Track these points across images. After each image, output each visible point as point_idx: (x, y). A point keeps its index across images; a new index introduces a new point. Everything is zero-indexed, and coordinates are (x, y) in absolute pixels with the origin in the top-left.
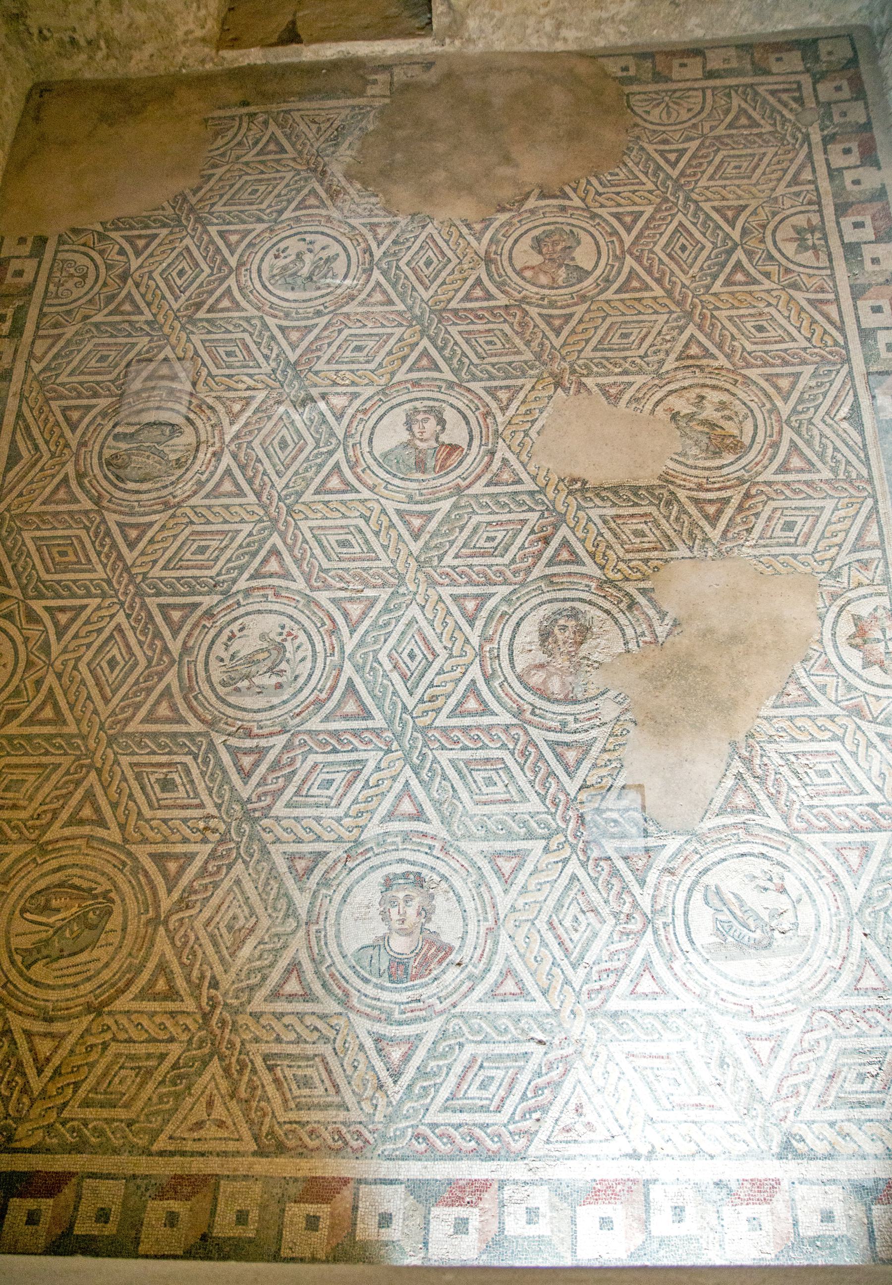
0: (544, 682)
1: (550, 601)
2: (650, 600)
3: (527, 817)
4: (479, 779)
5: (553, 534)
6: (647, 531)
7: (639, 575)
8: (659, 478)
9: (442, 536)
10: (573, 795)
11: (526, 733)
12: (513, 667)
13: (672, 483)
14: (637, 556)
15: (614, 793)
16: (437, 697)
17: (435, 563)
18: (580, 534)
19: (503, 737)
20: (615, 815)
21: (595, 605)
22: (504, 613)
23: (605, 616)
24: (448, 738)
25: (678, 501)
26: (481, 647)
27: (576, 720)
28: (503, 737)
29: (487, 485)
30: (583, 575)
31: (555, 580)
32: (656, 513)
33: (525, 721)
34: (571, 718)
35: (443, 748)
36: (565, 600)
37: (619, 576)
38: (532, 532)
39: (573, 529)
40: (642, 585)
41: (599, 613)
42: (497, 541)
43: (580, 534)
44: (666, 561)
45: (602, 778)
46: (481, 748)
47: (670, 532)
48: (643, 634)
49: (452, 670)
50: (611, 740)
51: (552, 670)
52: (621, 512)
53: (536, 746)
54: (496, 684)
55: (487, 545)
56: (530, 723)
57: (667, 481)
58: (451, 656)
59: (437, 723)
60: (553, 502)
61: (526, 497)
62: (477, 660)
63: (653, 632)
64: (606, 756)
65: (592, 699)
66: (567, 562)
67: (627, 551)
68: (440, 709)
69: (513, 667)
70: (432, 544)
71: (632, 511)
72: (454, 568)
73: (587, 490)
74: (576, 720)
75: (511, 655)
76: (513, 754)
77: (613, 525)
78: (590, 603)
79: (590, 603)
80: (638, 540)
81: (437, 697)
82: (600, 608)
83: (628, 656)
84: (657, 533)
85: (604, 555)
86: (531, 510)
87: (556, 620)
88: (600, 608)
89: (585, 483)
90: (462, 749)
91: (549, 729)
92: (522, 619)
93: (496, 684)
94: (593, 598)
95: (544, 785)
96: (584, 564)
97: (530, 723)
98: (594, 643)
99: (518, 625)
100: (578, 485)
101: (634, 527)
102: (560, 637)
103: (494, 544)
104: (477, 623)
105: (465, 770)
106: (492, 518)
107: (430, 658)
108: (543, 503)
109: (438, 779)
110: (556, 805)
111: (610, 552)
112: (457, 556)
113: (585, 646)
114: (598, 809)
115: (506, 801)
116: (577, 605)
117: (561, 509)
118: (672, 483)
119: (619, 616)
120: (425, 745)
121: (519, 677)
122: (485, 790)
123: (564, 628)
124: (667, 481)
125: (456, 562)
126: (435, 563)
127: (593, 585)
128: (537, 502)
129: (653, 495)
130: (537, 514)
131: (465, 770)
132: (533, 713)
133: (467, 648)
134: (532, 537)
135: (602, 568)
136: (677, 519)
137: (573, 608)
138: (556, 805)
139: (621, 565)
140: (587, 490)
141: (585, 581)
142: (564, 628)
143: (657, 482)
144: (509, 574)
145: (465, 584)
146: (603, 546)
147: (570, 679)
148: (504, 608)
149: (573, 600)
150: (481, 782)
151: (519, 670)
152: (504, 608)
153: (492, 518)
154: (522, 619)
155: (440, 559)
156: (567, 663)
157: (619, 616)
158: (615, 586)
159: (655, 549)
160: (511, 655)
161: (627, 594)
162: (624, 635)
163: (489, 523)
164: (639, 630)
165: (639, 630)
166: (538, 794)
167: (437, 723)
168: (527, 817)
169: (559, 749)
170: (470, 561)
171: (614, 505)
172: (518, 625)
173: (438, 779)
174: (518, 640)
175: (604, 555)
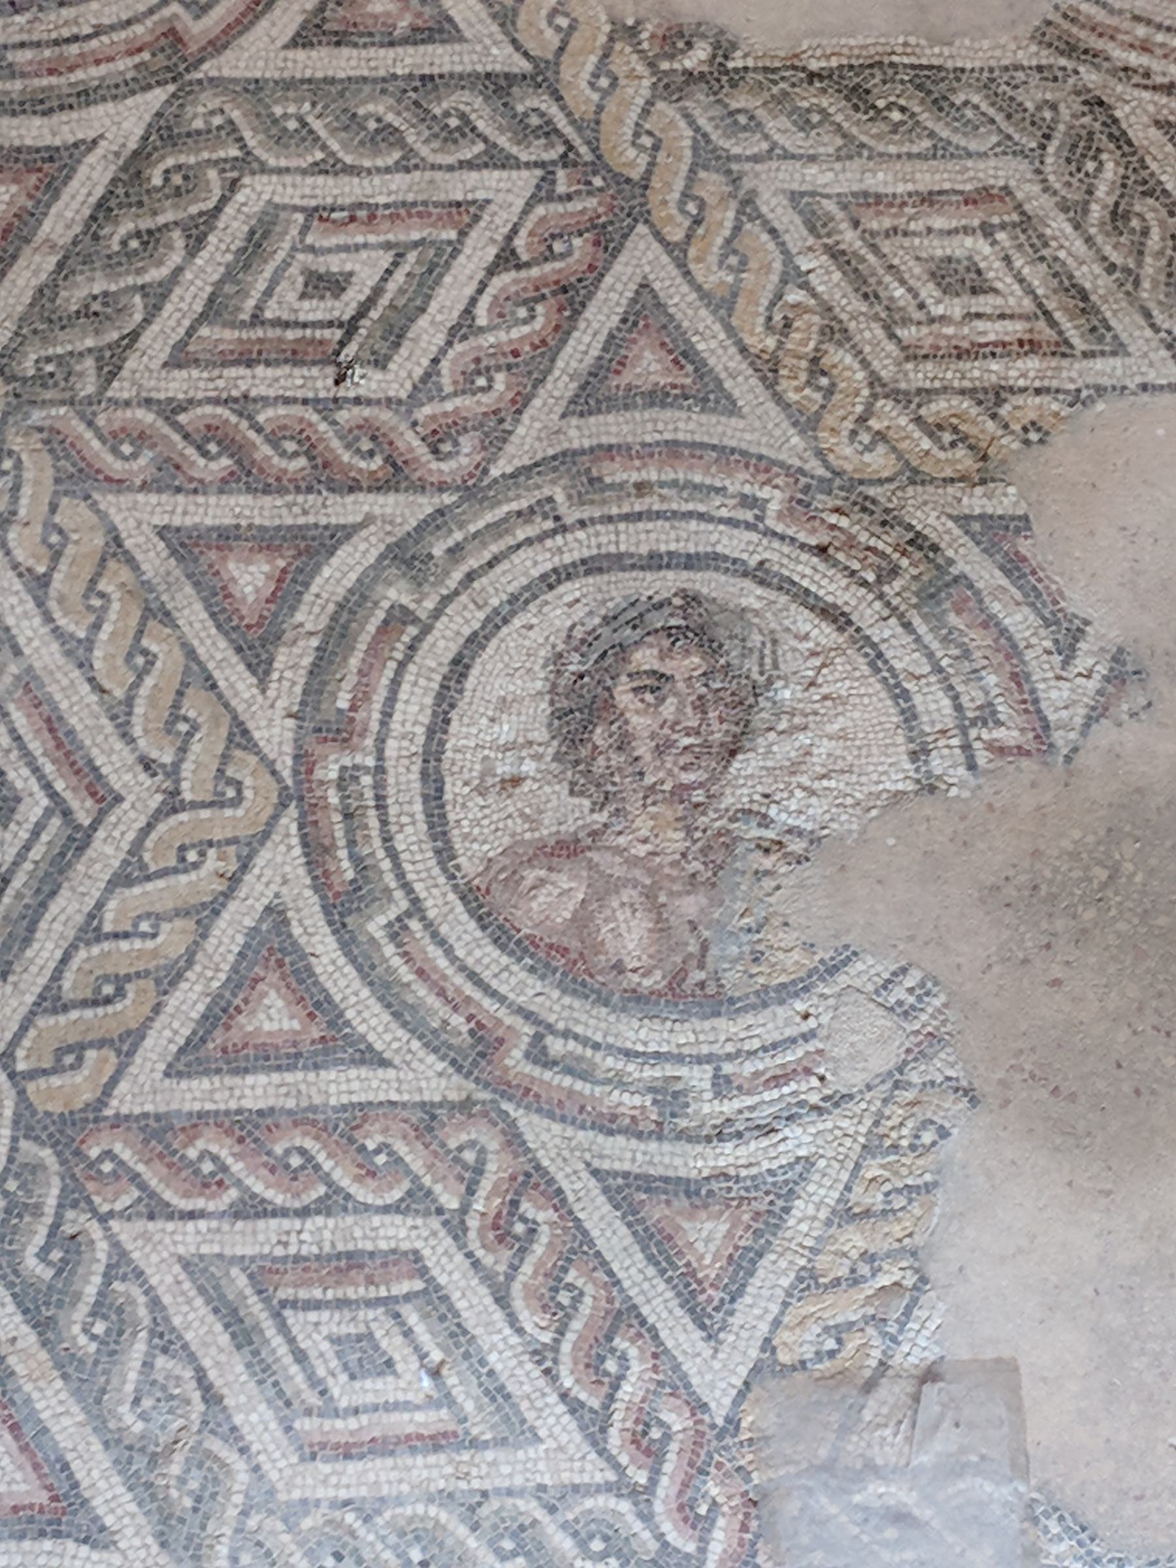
0: (582, 920)
1: (591, 566)
2: (1014, 567)
3: (531, 1508)
4: (317, 1344)
5: (596, 273)
6: (995, 271)
7: (963, 460)
8: (1040, 37)
9: (112, 265)
10: (720, 1408)
11: (514, 1140)
12: (445, 854)
13: (1092, 56)
14: (951, 375)
15: (890, 1393)
16: (121, 983)
17: (88, 387)
18: (713, 277)
19: (415, 1158)
20: (899, 1494)
21: (786, 585)
22: (400, 617)
23: (825, 634)
24: (176, 1165)
25: (1121, 139)
26: (304, 761)
27: (722, 1085)
28: (415, 1158)
29: (300, 41)
30: (726, 455)
31: (615, 473)
32: (1028, 191)
33: (505, 1088)
34: (699, 1078)
35: (156, 1209)
36: (655, 562)
37: (879, 461)
38: (506, 259)
39: (678, 252)
40: (976, 502)
41: (804, 620)
42: (354, 296)
43: (713, 277)
44: (1075, 399)
45: (839, 1332)
46: (323, 1207)
47: (1090, 275)
48: (988, 716)
49: (183, 866)
50: (872, 1169)
51: (614, 866)
52: (880, 180)
53: (557, 1198)
54: (376, 927)
55: (315, 310)
56: (526, 1094)
57: (1071, 49)
58: (173, 804)
59: (124, 1101)
60: (592, 126)
61: (473, 103)
62: (289, 821)
63: (1031, 706)
64: (854, 1240)
65: (786, 992)
66: (657, 398)
67: (911, 354)
68: (135, 1037)
69: (445, 854)
70: (73, 296)
71: (928, 177)
72: (171, 410)
73: (736, 78)
74: (722, 1085)
75: (434, 797)
76: (457, 1229)
77: (849, 238)
78: (761, 575)
79: (761, 575)
80: (955, 308)
81: (121, 983)
82: (804, 597)
83: (928, 807)
84: (1036, 276)
85: (816, 367)
86: (495, 159)
87: (623, 650)
88: (804, 597)
89: (723, 48)
90: (238, 1213)
91: (608, 1125)
92: (476, 642)
93: (376, 927)
94: (774, 554)
95: (594, 1365)
96: (732, 408)
97: (526, 1094)
98: (785, 750)
99: (460, 667)
100: (697, 57)
101: (939, 248)
102: (639, 722)
103: (345, 306)
104: (282, 658)
105: (255, 1307)
106: (327, 190)
107: (83, 810)
108: (549, 131)
109: (140, 1348)
110: (653, 1454)
111: (839, 357)
112: (180, 358)
113: (745, 765)
114: (828, 1467)
115: (436, 1442)
116: (704, 583)
117: (631, 160)
118: (1092, 56)
119: (886, 633)
120: (73, 1197)
121: (469, 896)
122: (342, 1391)
123: (657, 683)
124: (1071, 49)
125: (176, 385)
126: (88, 387)
127: (775, 499)
128: (522, 130)
129: (1013, 108)
130: (526, 180)
131: (255, 1307)
132: (538, 1055)
133: (244, 768)
134: (504, 280)
135: (808, 423)
136: (1118, 216)
137: (691, 599)
138: (653, 1454)
139: (889, 415)
140: (736, 78)
141: (739, 482)
142: (657, 683)
143: (1031, 54)
144: (411, 442)
145: (224, 485)
146: (808, 326)
147: (690, 905)
148: (397, 593)
149: (691, 562)
150: (326, 1362)
151: (468, 864)
152: (397, 593)
153: (327, 190)
154: (476, 642)
155: (110, 370)
156: (675, 840)
157: (886, 633)
158: (866, 506)
159: (1029, 346)
160: (434, 797)
161: (917, 541)
162: (909, 716)
163: (317, 214)
164: (971, 697)
165: (971, 697)
166: (575, 1407)
167: (124, 1101)
168: (531, 1508)
169: (656, 1212)
170: (241, 380)
171: (851, 149)
172: (460, 667)
173: (140, 1348)
174: (459, 734)
175: (816, 367)
